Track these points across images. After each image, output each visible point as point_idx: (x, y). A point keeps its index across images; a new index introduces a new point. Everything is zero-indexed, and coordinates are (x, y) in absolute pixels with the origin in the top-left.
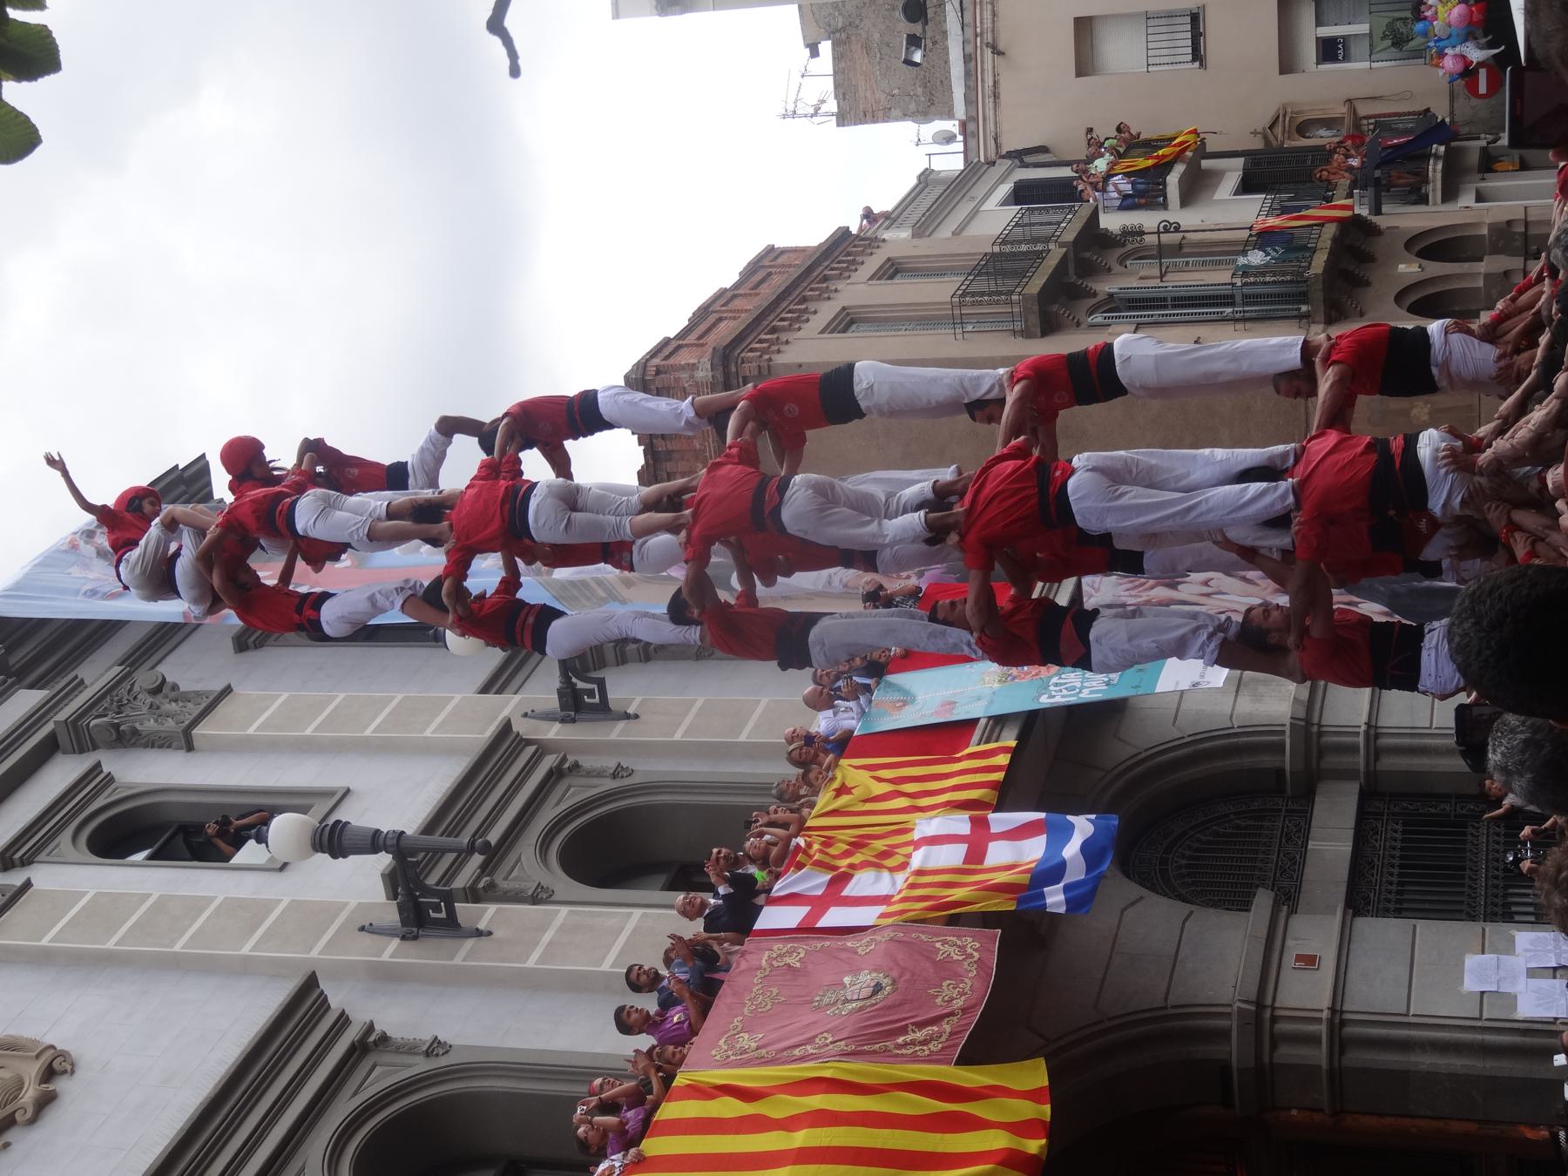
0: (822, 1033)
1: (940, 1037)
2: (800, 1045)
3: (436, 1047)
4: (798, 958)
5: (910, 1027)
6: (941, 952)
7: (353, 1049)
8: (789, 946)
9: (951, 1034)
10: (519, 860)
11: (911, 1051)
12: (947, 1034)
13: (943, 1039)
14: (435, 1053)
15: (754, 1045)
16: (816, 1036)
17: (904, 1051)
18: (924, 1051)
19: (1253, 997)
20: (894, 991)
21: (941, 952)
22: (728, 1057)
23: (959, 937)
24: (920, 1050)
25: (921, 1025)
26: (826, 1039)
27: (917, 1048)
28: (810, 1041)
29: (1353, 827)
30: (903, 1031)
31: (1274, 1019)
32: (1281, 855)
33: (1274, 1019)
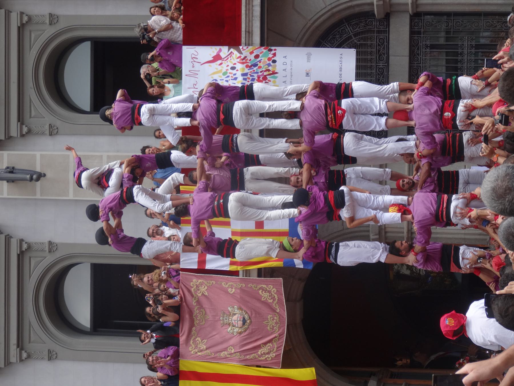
0: (229, 346)
1: (274, 350)
2: (223, 351)
3: (52, 246)
4: (205, 289)
5: (262, 345)
6: (263, 298)
7: (19, 255)
8: (200, 281)
9: (277, 348)
10: (30, 100)
11: (264, 358)
12: (276, 348)
13: (275, 351)
14: (52, 251)
15: (205, 347)
16: (227, 348)
17: (262, 358)
18: (269, 358)
19: (377, 232)
20: (251, 322)
21: (263, 298)
22: (196, 353)
23: (267, 285)
24: (268, 357)
25: (265, 344)
26: (232, 350)
27: (267, 356)
28: (225, 349)
29: (408, 55)
30: (259, 347)
31: (386, 232)
32: (377, 70)
33: (386, 232)
